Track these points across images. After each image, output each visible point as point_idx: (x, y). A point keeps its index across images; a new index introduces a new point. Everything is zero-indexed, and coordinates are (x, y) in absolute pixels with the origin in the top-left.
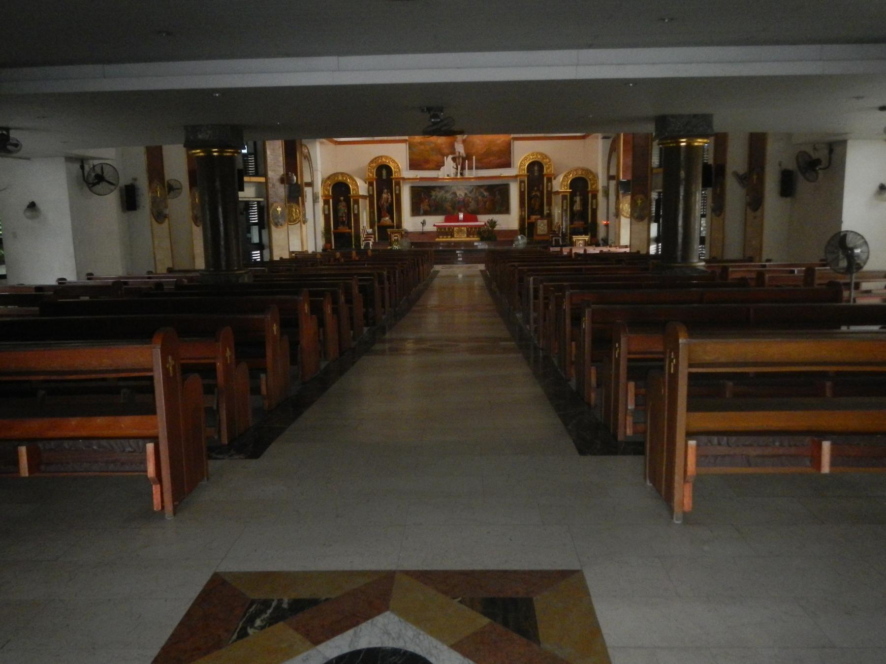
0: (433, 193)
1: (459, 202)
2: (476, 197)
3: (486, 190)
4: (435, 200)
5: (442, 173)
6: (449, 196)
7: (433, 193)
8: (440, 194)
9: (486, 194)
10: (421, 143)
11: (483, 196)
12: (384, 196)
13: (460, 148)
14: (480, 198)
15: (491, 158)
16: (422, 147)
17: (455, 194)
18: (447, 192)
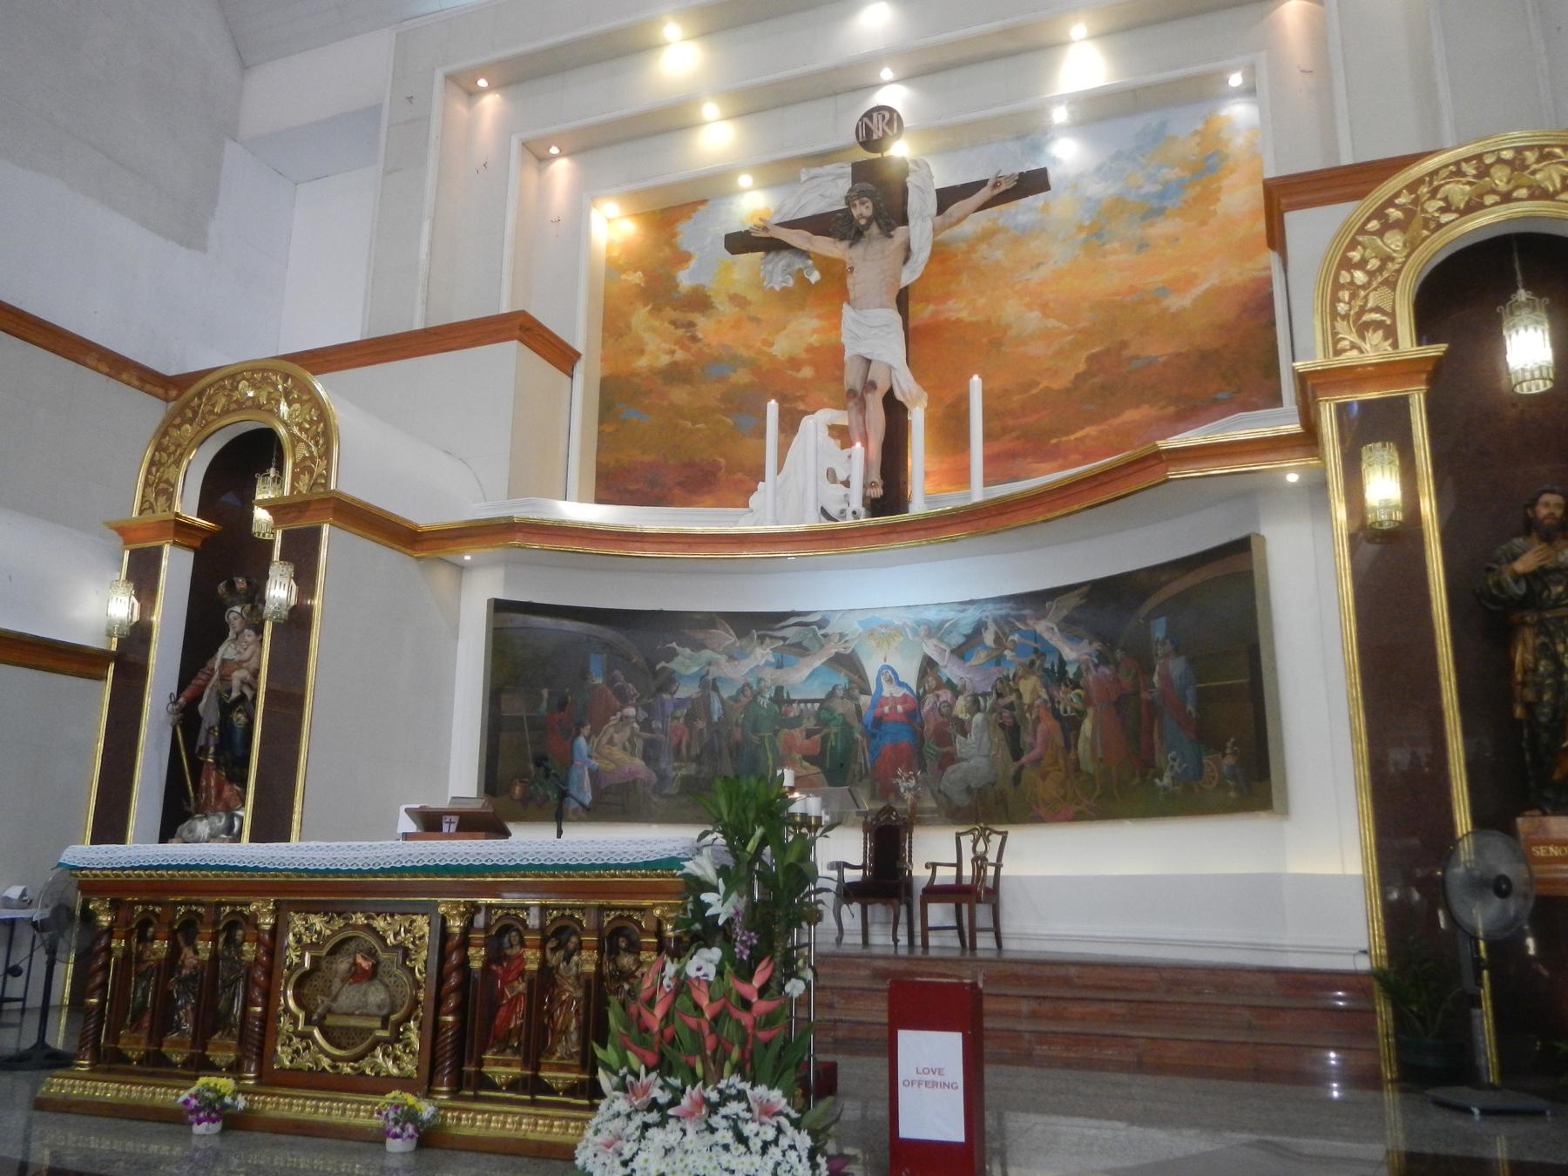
0: (686, 663)
1: (879, 721)
2: (1005, 686)
3: (1069, 626)
4: (698, 708)
5: (762, 513)
6: (806, 680)
7: (686, 663)
8: (753, 664)
9: (1073, 653)
10: (676, 374)
11: (1057, 676)
12: (226, 651)
13: (874, 338)
14: (1029, 687)
15: (1130, 415)
16: (679, 395)
17: (847, 663)
18: (801, 650)
